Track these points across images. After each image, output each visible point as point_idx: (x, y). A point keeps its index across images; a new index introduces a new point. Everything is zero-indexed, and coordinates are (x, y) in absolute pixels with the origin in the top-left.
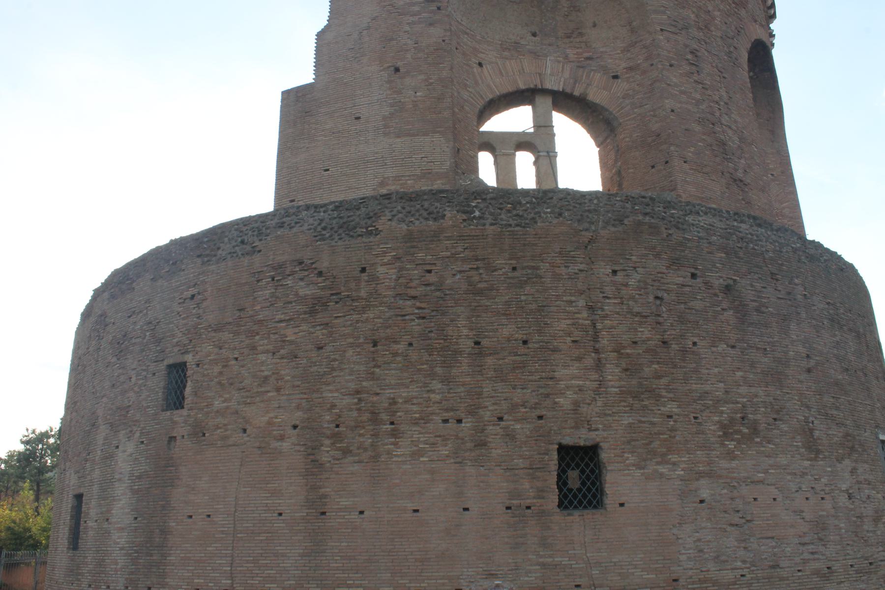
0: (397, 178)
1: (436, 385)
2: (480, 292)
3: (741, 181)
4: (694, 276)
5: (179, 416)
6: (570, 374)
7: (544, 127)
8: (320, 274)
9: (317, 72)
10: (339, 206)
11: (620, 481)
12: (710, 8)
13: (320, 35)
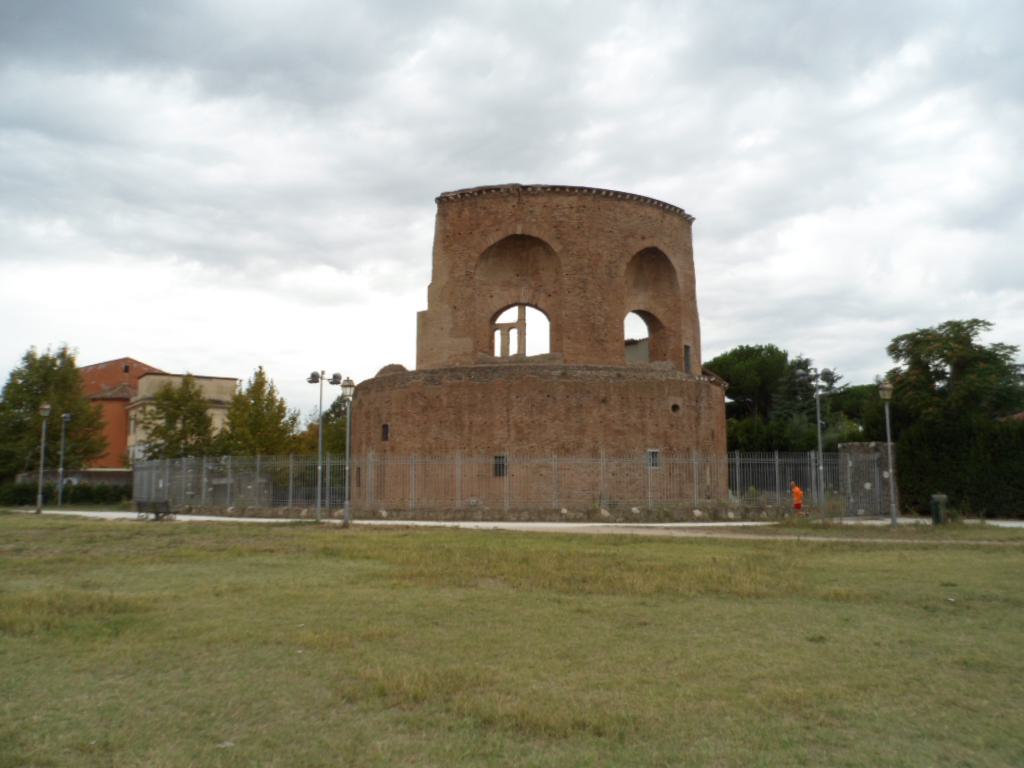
1: (459, 437)
3: (603, 341)
4: (548, 396)
5: (387, 443)
6: (500, 433)
9: (429, 306)
10: (432, 372)
11: (515, 468)
12: (600, 251)
13: (429, 287)
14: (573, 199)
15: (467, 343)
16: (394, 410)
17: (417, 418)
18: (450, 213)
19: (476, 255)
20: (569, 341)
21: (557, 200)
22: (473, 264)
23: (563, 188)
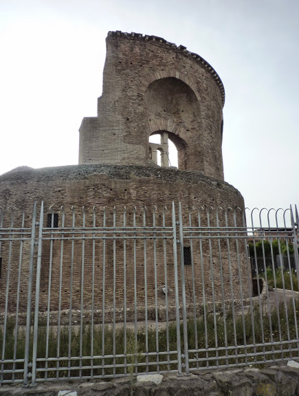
0: (128, 158)
2: (161, 201)
7: (165, 143)
8: (111, 190)
10: (115, 167)
13: (99, 99)
14: (202, 70)
15: (141, 150)
16: (69, 199)
17: (101, 208)
18: (123, 46)
19: (147, 84)
20: (207, 164)
21: (197, 67)
22: (144, 89)
23: (202, 59)
